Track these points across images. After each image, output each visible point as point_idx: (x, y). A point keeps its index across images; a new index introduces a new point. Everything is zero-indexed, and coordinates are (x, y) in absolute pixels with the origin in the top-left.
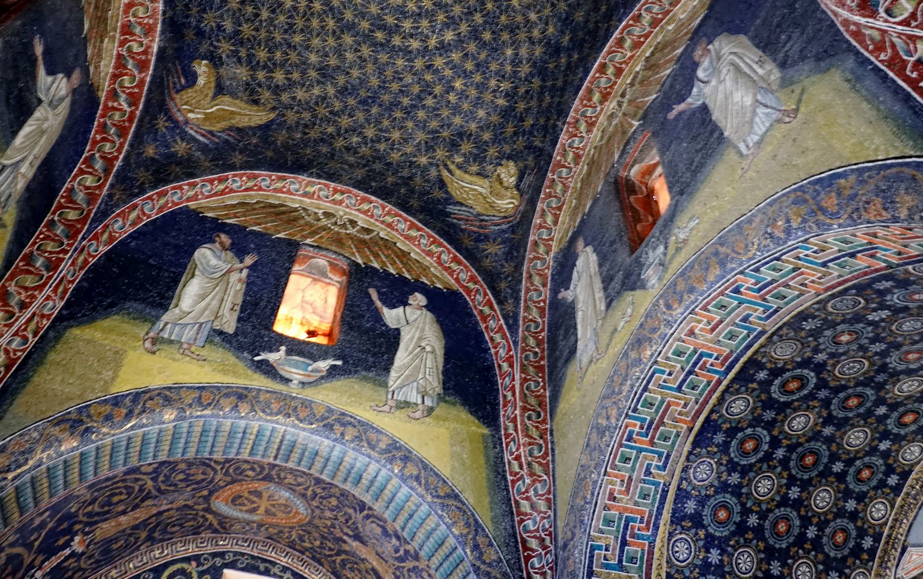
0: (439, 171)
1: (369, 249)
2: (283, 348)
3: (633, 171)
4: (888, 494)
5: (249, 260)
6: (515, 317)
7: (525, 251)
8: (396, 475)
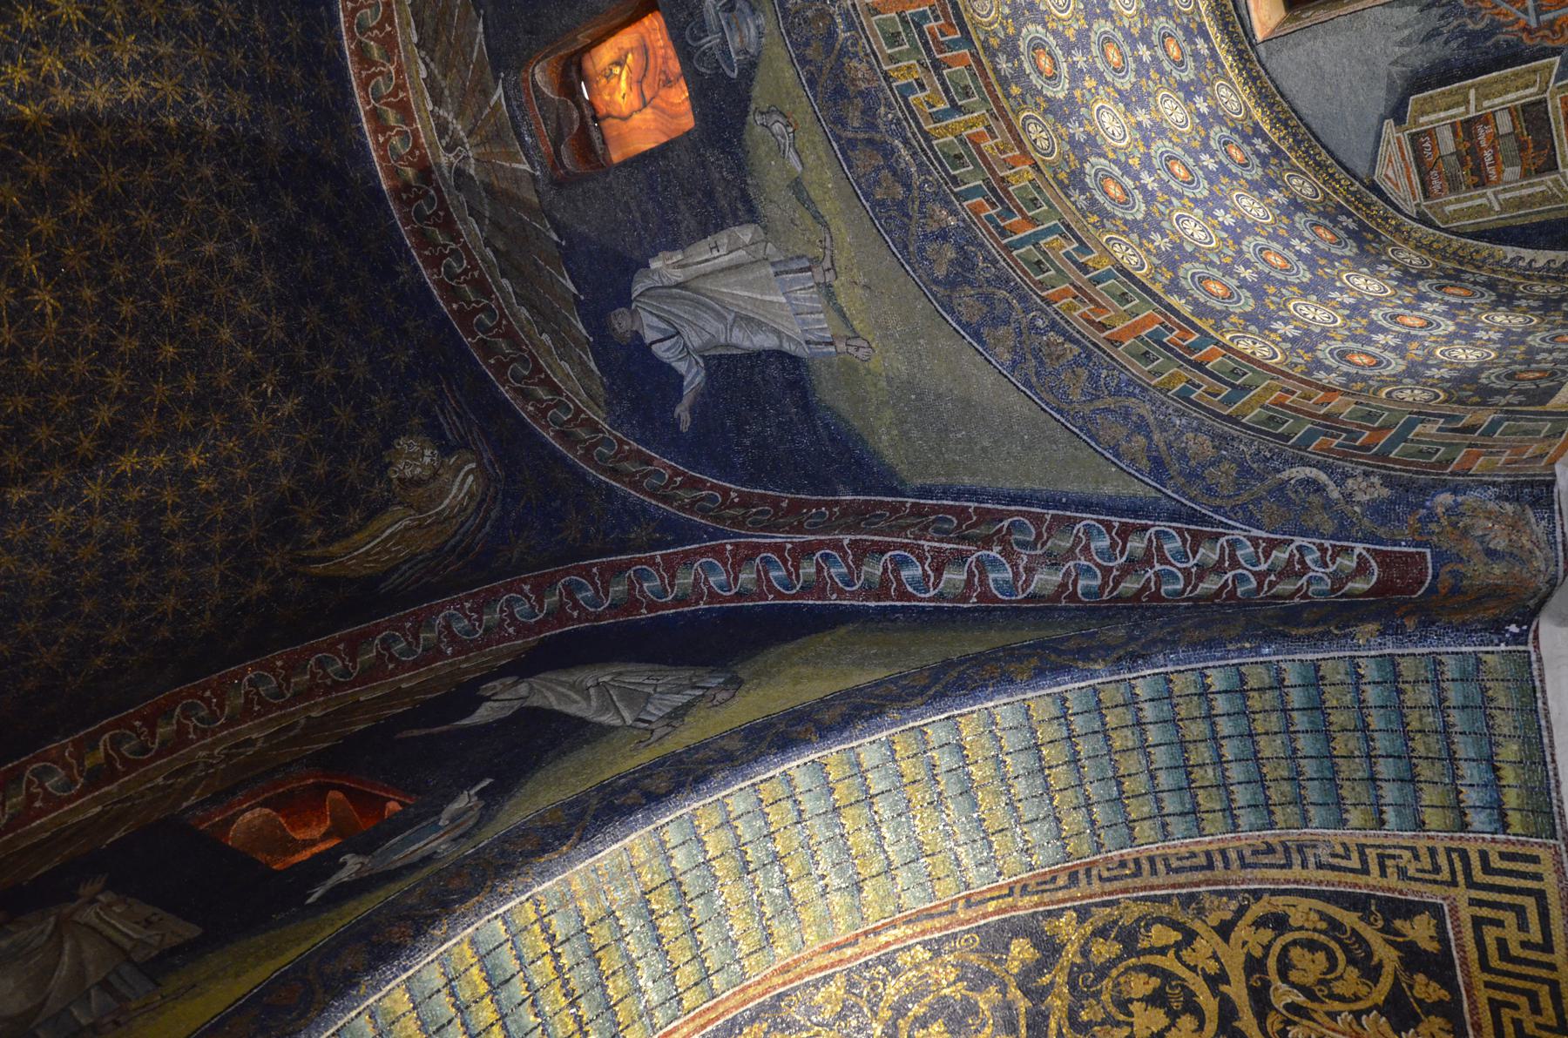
3: (566, 161)
7: (564, 458)
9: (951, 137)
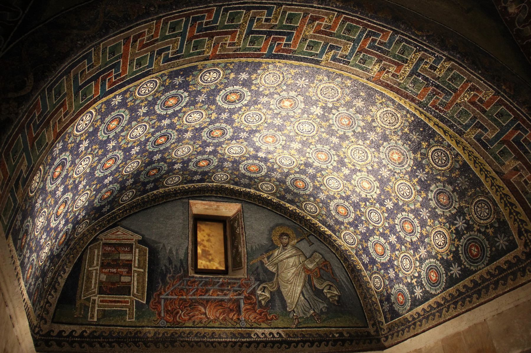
4: (139, 191)
9: (241, 21)
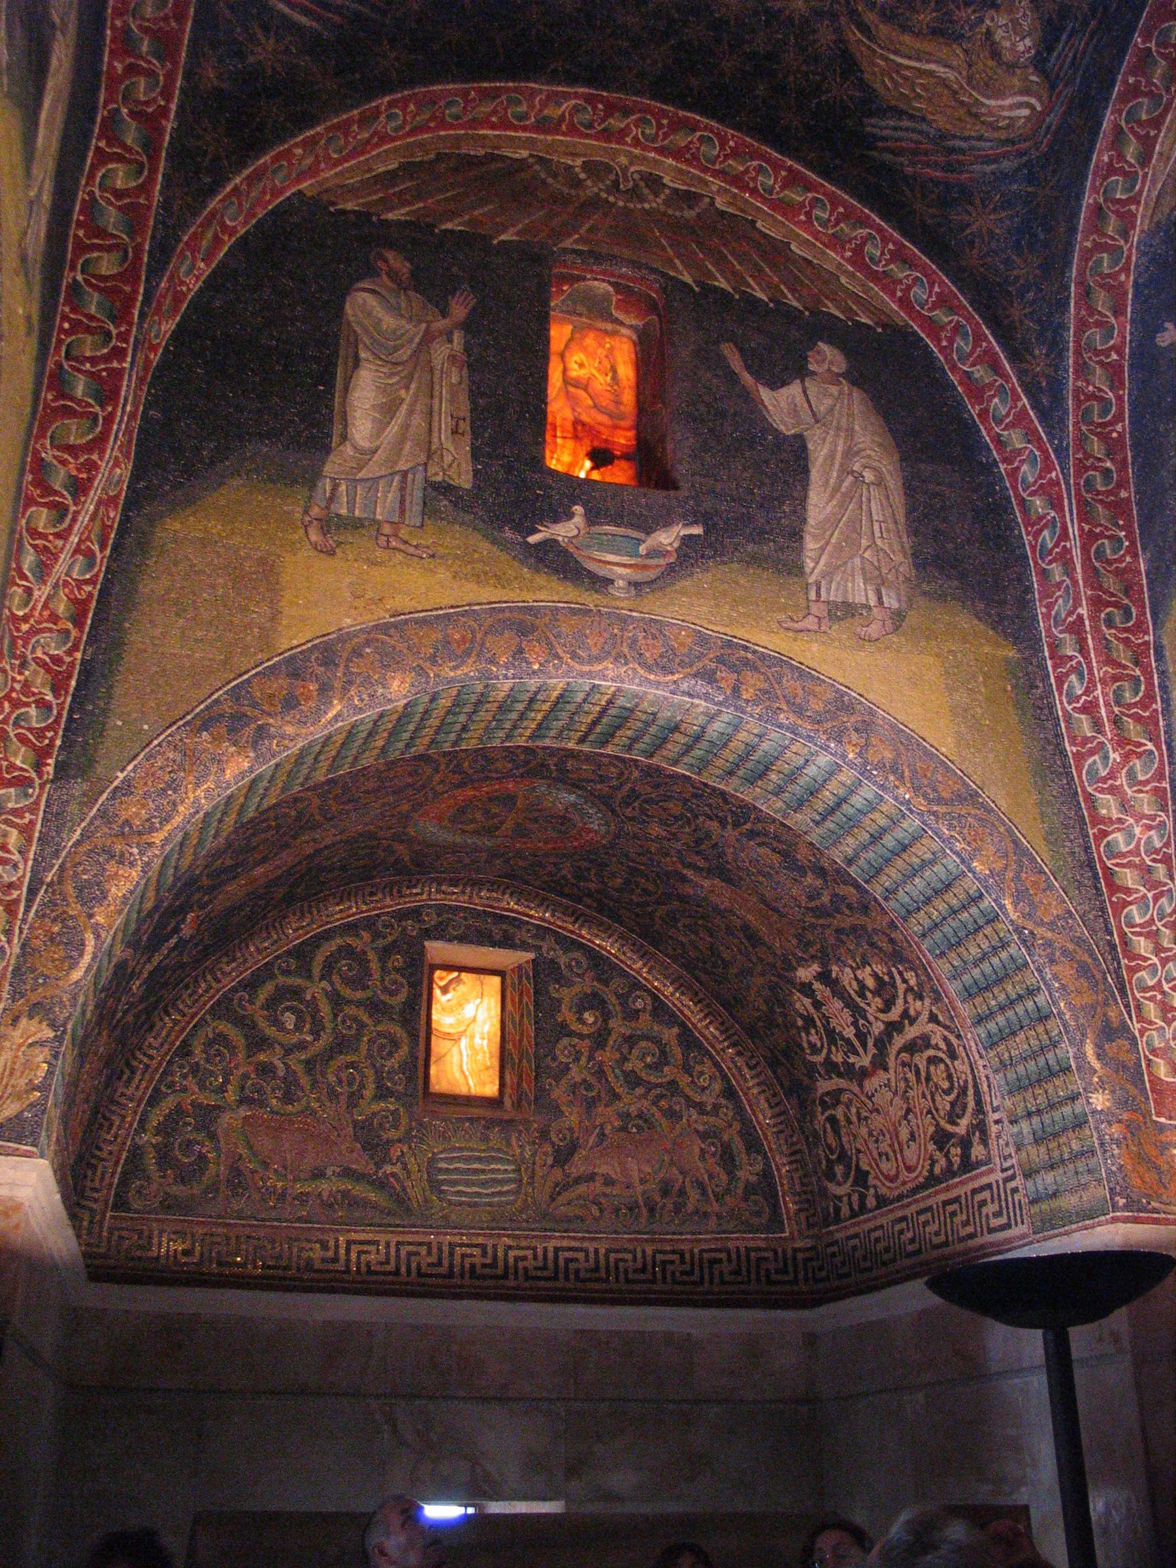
0: (838, 31)
1: (698, 243)
2: (578, 509)
5: (459, 310)
6: (1056, 388)
7: (1073, 230)
8: (851, 765)
